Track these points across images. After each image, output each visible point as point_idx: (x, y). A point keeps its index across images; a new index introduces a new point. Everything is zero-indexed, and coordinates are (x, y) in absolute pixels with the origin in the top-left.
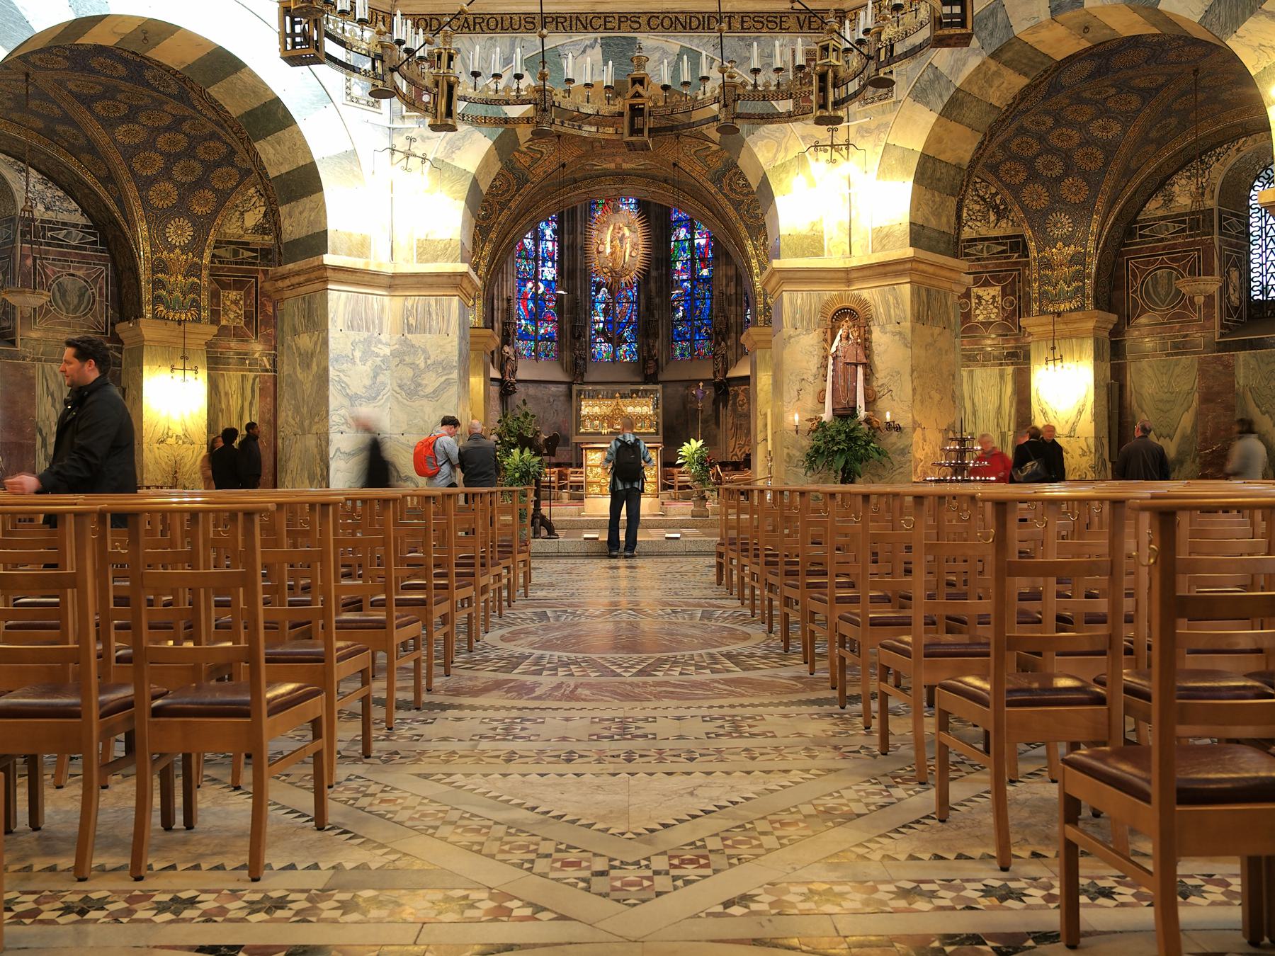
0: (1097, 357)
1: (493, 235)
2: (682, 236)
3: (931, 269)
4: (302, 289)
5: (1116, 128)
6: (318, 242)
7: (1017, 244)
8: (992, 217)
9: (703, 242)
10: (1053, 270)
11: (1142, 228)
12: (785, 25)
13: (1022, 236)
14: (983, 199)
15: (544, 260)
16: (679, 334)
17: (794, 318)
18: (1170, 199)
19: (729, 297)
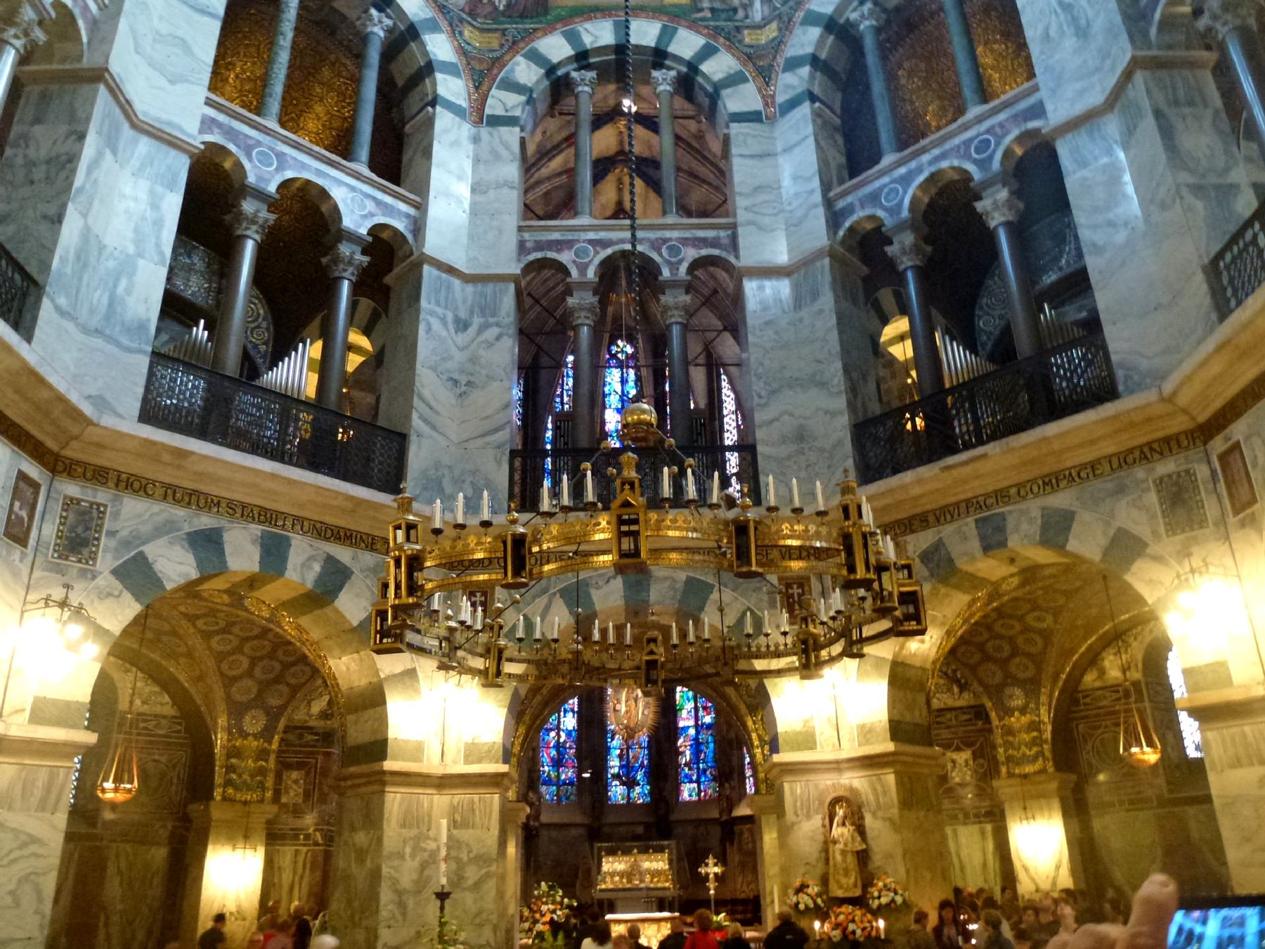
0: (1066, 816)
1: (527, 718)
3: (910, 759)
4: (363, 790)
5: (1049, 620)
6: (379, 748)
7: (979, 713)
8: (956, 690)
10: (1014, 736)
11: (1084, 697)
12: (770, 557)
13: (982, 706)
14: (946, 674)
15: (565, 711)
16: (686, 776)
17: (795, 806)
18: (1102, 672)
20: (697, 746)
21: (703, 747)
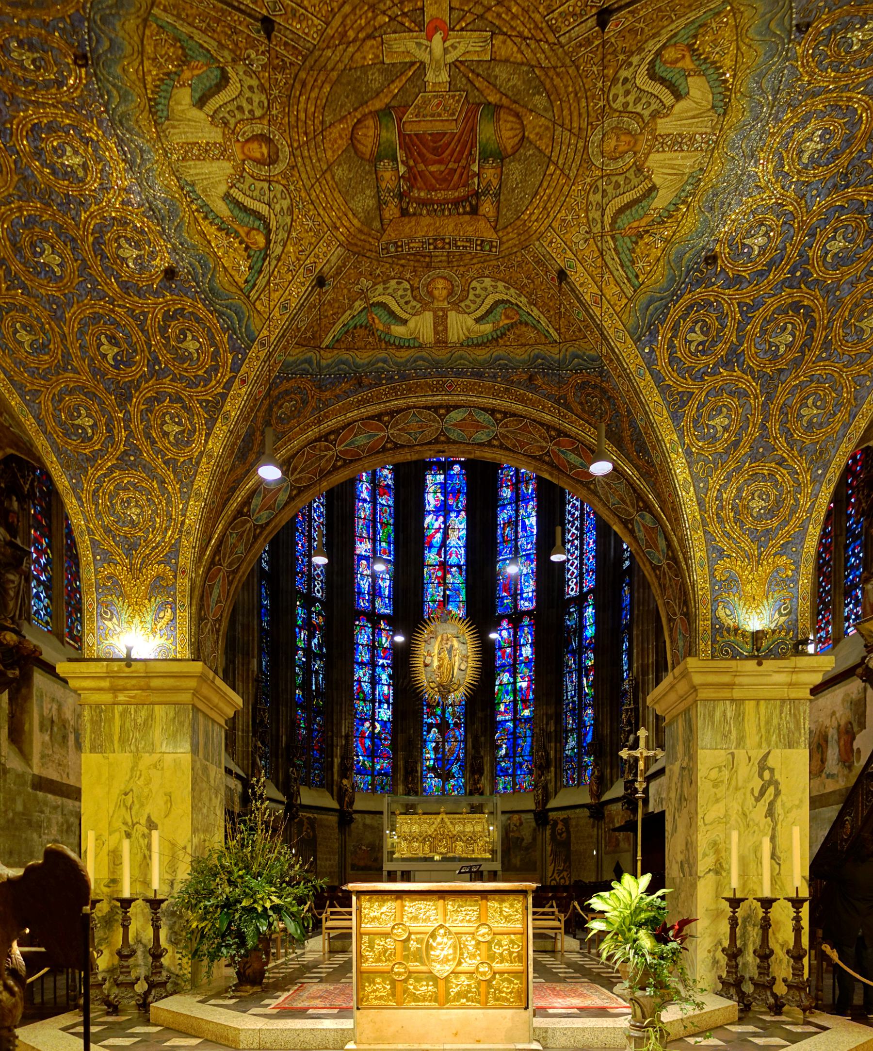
2: (505, 681)
9: (524, 685)
15: (380, 702)
16: (502, 769)
19: (548, 735)
20: (514, 738)
21: (520, 741)
